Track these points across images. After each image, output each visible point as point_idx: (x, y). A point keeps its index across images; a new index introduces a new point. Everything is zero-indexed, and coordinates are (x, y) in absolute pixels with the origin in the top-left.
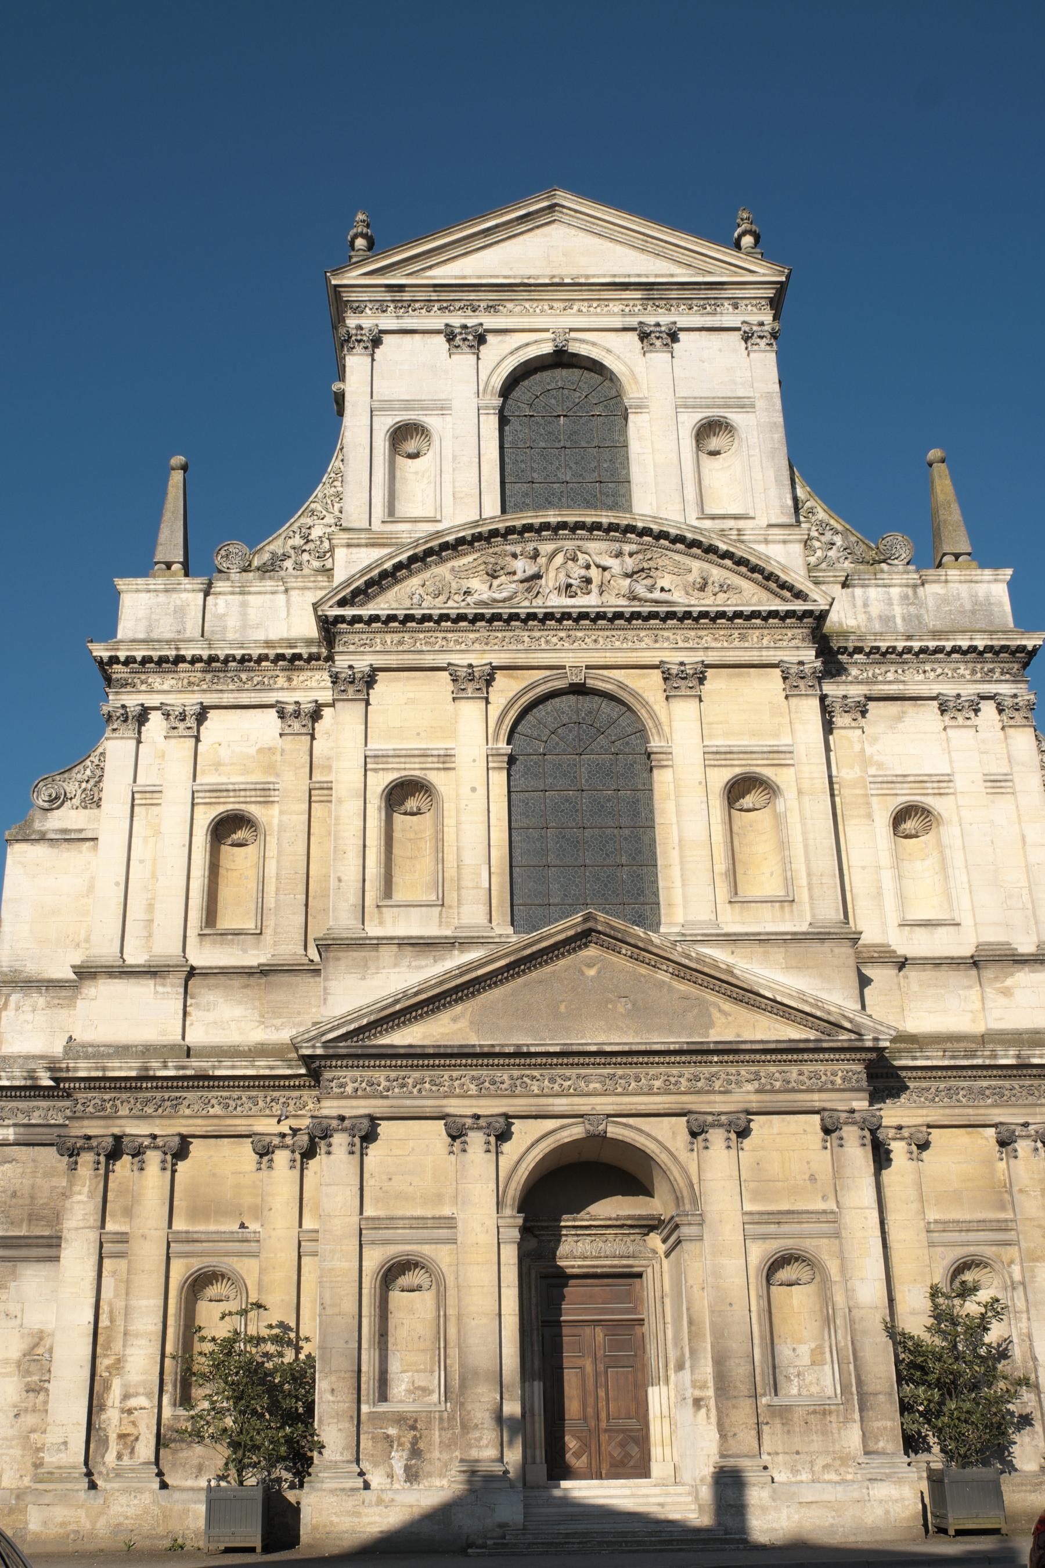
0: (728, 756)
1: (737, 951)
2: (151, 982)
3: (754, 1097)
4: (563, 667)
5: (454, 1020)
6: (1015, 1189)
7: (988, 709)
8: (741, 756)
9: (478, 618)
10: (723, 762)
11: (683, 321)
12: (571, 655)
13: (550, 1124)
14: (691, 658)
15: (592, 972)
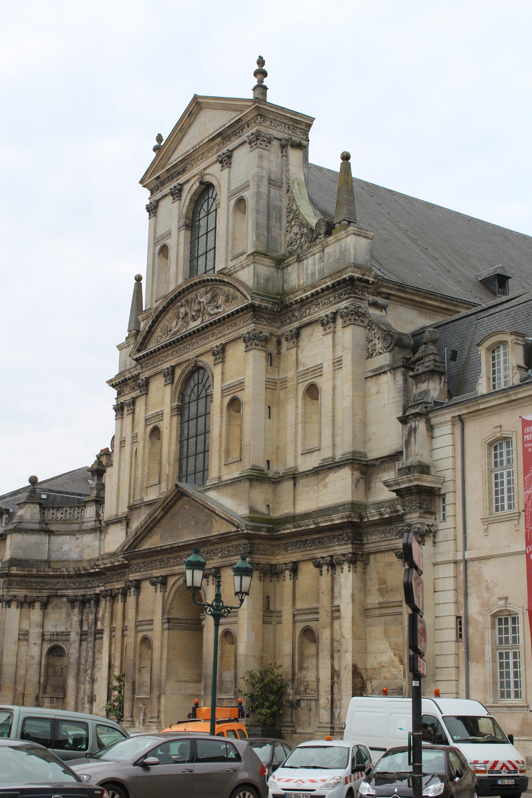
0: (230, 389)
1: (220, 490)
2: (119, 525)
3: (220, 560)
4: (189, 360)
5: (157, 535)
6: (320, 591)
7: (340, 321)
8: (233, 388)
9: (166, 346)
10: (228, 393)
11: (231, 146)
12: (191, 353)
13: (177, 577)
14: (218, 343)
15: (187, 507)
